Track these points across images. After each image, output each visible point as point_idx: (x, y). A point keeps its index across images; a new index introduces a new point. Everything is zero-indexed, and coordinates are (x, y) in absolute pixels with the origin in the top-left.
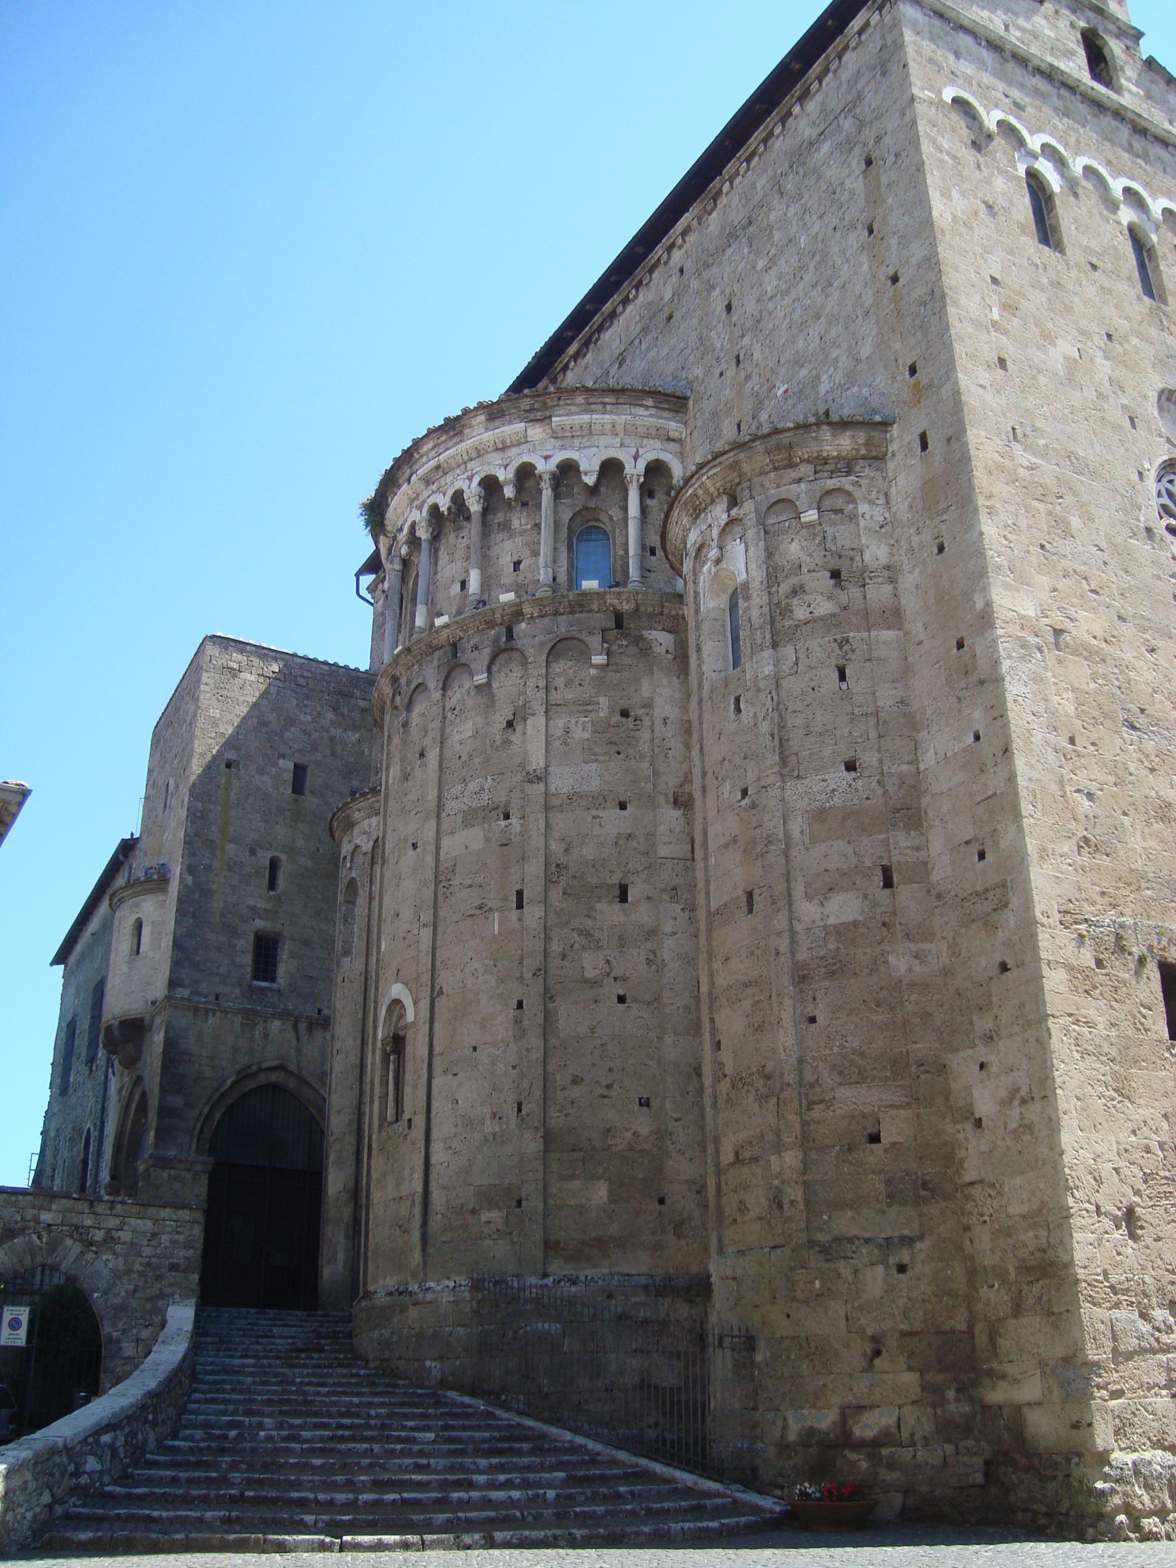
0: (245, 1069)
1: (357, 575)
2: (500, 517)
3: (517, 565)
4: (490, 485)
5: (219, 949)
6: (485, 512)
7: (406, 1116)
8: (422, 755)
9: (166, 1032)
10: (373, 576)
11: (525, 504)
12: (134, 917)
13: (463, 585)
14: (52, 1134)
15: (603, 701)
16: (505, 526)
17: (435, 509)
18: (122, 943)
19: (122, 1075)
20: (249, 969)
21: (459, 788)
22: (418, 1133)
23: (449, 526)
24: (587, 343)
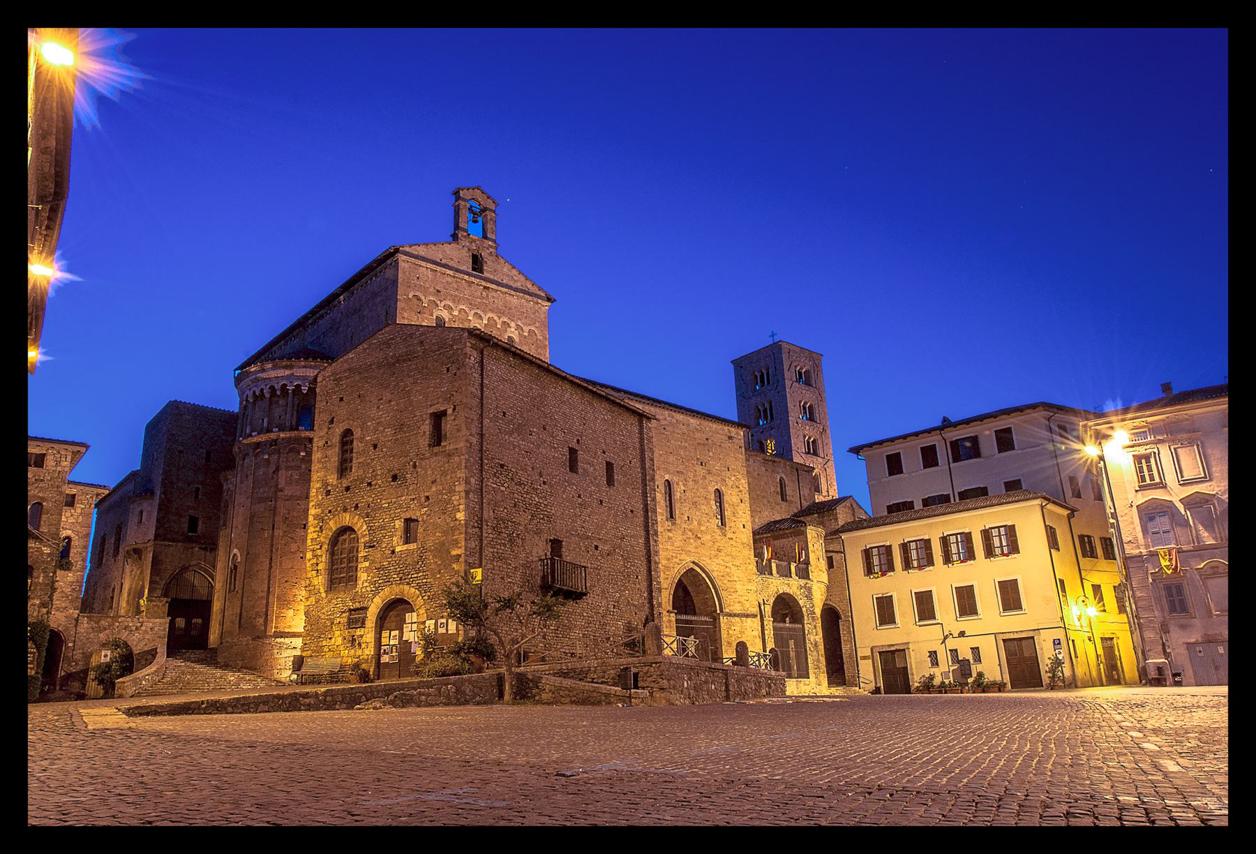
0: (184, 566)
1: (237, 369)
2: (275, 399)
3: (280, 417)
4: (272, 388)
5: (174, 522)
6: (271, 396)
7: (236, 590)
8: (247, 477)
9: (153, 553)
10: (240, 371)
11: (284, 396)
12: (139, 509)
13: (263, 421)
14: (92, 584)
15: (303, 466)
16: (277, 402)
17: (254, 392)
18: (134, 519)
19: (132, 565)
20: (186, 529)
21: (258, 490)
22: (239, 595)
23: (259, 399)
24: (315, 322)
